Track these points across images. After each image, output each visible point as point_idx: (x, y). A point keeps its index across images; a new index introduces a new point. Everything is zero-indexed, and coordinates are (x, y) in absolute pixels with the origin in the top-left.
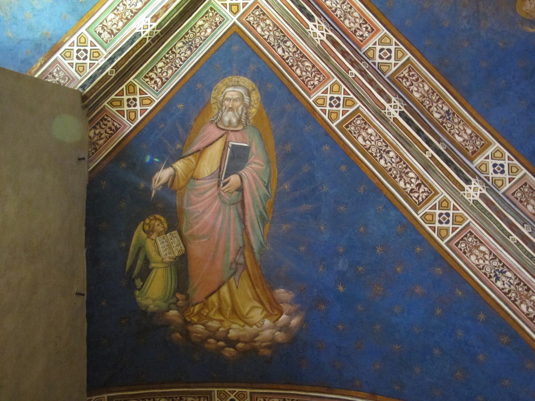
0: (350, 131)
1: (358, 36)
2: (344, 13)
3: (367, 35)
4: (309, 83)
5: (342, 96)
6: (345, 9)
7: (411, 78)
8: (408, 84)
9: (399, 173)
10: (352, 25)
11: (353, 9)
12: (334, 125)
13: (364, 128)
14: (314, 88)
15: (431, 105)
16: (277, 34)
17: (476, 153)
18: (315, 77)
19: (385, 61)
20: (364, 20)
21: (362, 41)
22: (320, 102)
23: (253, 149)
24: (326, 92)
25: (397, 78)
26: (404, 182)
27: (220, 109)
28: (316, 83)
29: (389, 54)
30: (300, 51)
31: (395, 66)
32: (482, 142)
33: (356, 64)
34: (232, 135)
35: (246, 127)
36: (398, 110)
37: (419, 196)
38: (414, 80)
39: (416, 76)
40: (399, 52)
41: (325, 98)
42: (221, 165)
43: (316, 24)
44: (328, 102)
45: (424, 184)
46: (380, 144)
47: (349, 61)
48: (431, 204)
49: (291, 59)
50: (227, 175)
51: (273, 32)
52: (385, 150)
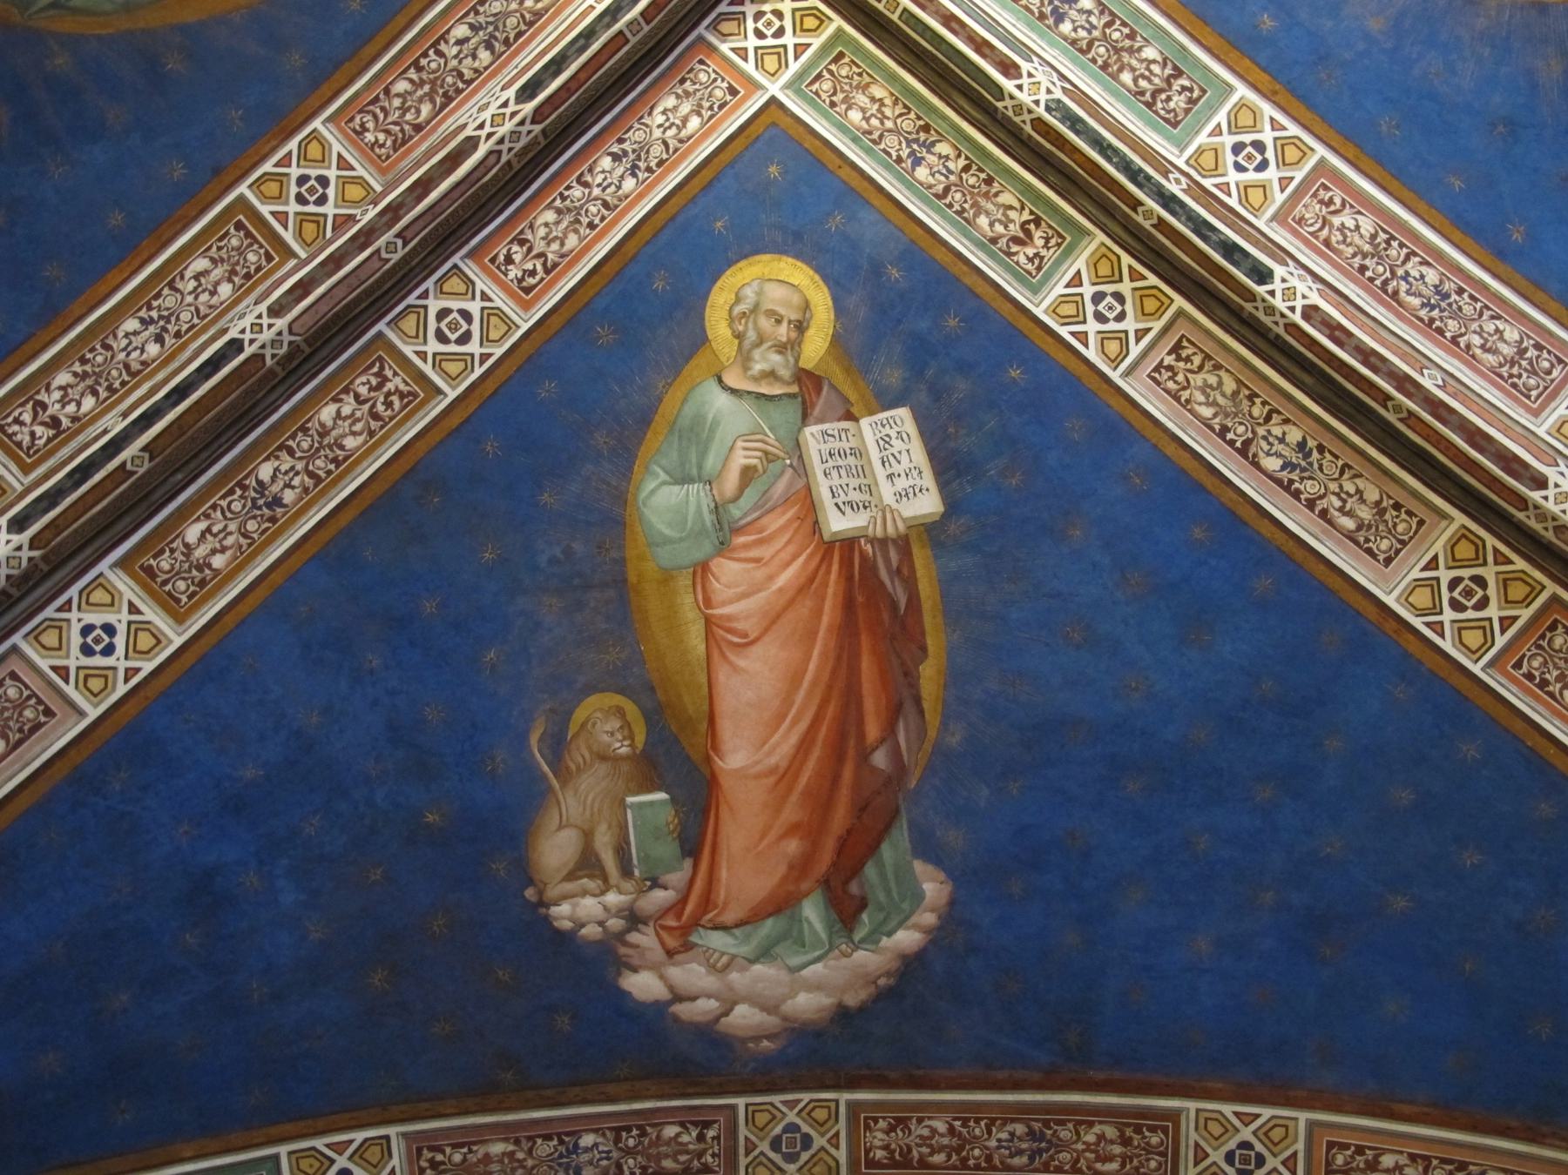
0: (227, 233)
1: (510, 249)
2: (575, 207)
3: (512, 275)
4: (369, 117)
6: (587, 211)
7: (382, 399)
8: (363, 390)
9: (97, 370)
10: (542, 232)
11: (588, 231)
12: (243, 189)
13: (233, 272)
14: (354, 130)
15: (298, 454)
16: (512, 21)
17: (147, 578)
18: (388, 132)
19: (432, 324)
20: (555, 265)
21: (493, 260)
22: (314, 150)
24: (342, 164)
25: (380, 359)
26: (69, 385)
28: (369, 137)
29: (453, 337)
30: (463, 90)
31: (417, 353)
32: (184, 599)
33: (391, 219)
36: (247, 336)
37: (22, 424)
38: (374, 406)
39: (389, 412)
40: (461, 365)
41: (326, 163)
43: (512, 107)
44: (314, 173)
45: (55, 436)
46: (185, 316)
47: (400, 199)
49: (440, 65)
51: (516, 11)
52: (166, 331)
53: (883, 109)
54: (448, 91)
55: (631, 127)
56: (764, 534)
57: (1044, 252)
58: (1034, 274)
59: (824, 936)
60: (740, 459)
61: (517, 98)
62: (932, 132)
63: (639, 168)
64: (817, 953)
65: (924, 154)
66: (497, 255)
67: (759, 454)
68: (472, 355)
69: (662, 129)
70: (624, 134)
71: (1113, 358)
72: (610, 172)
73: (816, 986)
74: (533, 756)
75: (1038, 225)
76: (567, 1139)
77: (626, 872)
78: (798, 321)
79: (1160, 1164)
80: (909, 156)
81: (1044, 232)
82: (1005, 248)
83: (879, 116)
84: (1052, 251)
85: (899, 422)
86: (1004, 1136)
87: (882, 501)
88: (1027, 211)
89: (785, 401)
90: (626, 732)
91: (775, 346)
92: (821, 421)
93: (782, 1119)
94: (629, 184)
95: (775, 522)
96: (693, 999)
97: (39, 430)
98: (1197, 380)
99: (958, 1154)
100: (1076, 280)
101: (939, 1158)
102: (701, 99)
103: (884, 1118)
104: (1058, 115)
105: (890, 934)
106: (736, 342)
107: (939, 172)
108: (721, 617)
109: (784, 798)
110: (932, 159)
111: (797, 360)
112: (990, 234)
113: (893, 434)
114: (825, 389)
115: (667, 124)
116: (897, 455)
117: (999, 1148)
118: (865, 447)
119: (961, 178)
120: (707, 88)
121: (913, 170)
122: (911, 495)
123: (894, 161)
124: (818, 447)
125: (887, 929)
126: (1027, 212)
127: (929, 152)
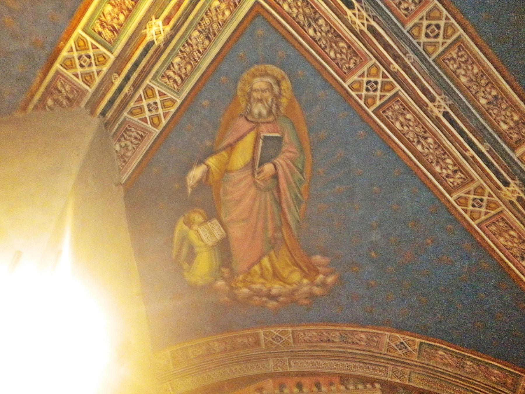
5: (380, 80)
7: (460, 59)
8: (455, 66)
12: (370, 111)
16: (307, 11)
18: (350, 59)
22: (356, 86)
23: (286, 139)
27: (249, 101)
28: (352, 66)
34: (263, 127)
35: (278, 117)
36: (442, 110)
38: (462, 62)
39: (466, 57)
40: (450, 28)
42: (253, 158)
44: (365, 85)
48: (466, 189)
50: (261, 165)
97: (458, 176)
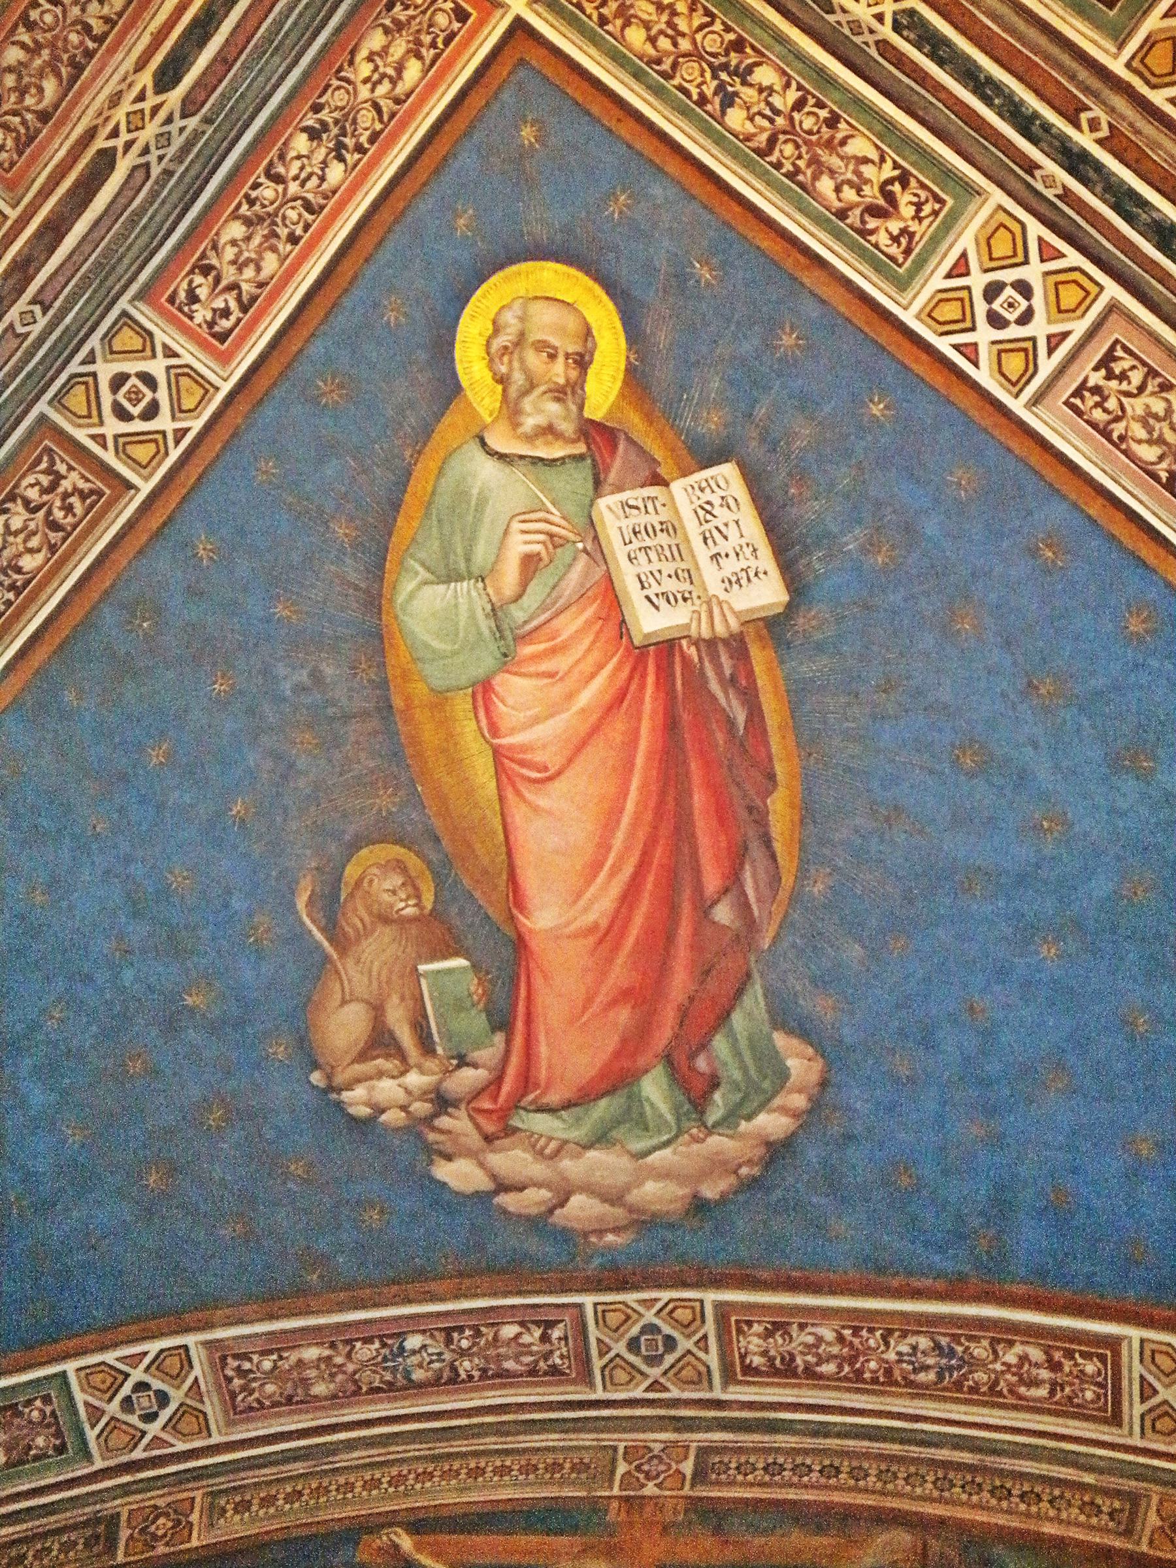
1: (191, 282)
2: (269, 215)
3: (198, 318)
6: (284, 218)
7: (58, 503)
8: (33, 494)
10: (230, 253)
11: (289, 247)
20: (254, 299)
21: (172, 300)
29: (136, 411)
30: (95, 51)
31: (93, 437)
38: (49, 513)
39: (70, 519)
40: (152, 448)
49: (56, 16)
53: (676, 20)
54: (75, 56)
55: (328, 86)
56: (559, 640)
57: (914, 226)
58: (901, 260)
59: (669, 1117)
60: (518, 546)
61: (156, 85)
62: (748, 50)
63: (345, 147)
64: (665, 1138)
65: (738, 87)
66: (175, 292)
67: (542, 537)
68: (164, 433)
69: (369, 86)
70: (320, 96)
71: (1014, 379)
72: (308, 157)
73: (664, 1174)
74: (302, 924)
75: (905, 185)
76: (390, 1342)
77: (426, 1046)
78: (577, 354)
79: (1098, 1396)
80: (715, 93)
81: (915, 195)
82: (858, 224)
83: (670, 32)
84: (926, 222)
85: (722, 484)
86: (905, 1349)
87: (705, 590)
88: (889, 163)
89: (570, 466)
90: (410, 889)
91: (550, 391)
92: (620, 489)
93: (637, 1321)
94: (336, 172)
95: (570, 624)
96: (521, 1188)
98: (1136, 406)
99: (851, 1364)
100: (961, 268)
101: (829, 1368)
102: (418, 31)
103: (759, 1322)
104: (912, 36)
105: (749, 1118)
106: (500, 388)
107: (760, 113)
108: (511, 747)
109: (610, 961)
110: (749, 94)
111: (581, 408)
112: (837, 204)
113: (717, 501)
114: (621, 447)
115: (376, 77)
116: (723, 528)
117: (900, 1361)
118: (680, 519)
119: (791, 119)
120: (424, 12)
121: (723, 113)
122: (744, 582)
123: (695, 103)
124: (618, 524)
125: (745, 1111)
126: (889, 164)
127: (744, 83)
